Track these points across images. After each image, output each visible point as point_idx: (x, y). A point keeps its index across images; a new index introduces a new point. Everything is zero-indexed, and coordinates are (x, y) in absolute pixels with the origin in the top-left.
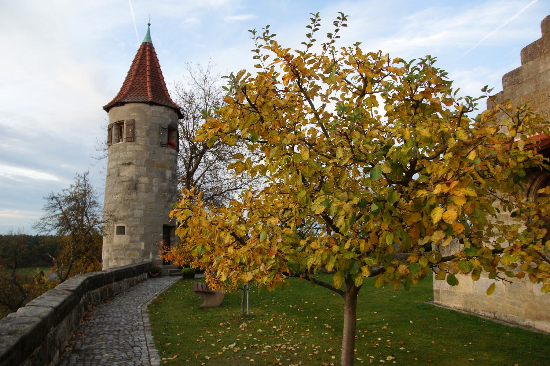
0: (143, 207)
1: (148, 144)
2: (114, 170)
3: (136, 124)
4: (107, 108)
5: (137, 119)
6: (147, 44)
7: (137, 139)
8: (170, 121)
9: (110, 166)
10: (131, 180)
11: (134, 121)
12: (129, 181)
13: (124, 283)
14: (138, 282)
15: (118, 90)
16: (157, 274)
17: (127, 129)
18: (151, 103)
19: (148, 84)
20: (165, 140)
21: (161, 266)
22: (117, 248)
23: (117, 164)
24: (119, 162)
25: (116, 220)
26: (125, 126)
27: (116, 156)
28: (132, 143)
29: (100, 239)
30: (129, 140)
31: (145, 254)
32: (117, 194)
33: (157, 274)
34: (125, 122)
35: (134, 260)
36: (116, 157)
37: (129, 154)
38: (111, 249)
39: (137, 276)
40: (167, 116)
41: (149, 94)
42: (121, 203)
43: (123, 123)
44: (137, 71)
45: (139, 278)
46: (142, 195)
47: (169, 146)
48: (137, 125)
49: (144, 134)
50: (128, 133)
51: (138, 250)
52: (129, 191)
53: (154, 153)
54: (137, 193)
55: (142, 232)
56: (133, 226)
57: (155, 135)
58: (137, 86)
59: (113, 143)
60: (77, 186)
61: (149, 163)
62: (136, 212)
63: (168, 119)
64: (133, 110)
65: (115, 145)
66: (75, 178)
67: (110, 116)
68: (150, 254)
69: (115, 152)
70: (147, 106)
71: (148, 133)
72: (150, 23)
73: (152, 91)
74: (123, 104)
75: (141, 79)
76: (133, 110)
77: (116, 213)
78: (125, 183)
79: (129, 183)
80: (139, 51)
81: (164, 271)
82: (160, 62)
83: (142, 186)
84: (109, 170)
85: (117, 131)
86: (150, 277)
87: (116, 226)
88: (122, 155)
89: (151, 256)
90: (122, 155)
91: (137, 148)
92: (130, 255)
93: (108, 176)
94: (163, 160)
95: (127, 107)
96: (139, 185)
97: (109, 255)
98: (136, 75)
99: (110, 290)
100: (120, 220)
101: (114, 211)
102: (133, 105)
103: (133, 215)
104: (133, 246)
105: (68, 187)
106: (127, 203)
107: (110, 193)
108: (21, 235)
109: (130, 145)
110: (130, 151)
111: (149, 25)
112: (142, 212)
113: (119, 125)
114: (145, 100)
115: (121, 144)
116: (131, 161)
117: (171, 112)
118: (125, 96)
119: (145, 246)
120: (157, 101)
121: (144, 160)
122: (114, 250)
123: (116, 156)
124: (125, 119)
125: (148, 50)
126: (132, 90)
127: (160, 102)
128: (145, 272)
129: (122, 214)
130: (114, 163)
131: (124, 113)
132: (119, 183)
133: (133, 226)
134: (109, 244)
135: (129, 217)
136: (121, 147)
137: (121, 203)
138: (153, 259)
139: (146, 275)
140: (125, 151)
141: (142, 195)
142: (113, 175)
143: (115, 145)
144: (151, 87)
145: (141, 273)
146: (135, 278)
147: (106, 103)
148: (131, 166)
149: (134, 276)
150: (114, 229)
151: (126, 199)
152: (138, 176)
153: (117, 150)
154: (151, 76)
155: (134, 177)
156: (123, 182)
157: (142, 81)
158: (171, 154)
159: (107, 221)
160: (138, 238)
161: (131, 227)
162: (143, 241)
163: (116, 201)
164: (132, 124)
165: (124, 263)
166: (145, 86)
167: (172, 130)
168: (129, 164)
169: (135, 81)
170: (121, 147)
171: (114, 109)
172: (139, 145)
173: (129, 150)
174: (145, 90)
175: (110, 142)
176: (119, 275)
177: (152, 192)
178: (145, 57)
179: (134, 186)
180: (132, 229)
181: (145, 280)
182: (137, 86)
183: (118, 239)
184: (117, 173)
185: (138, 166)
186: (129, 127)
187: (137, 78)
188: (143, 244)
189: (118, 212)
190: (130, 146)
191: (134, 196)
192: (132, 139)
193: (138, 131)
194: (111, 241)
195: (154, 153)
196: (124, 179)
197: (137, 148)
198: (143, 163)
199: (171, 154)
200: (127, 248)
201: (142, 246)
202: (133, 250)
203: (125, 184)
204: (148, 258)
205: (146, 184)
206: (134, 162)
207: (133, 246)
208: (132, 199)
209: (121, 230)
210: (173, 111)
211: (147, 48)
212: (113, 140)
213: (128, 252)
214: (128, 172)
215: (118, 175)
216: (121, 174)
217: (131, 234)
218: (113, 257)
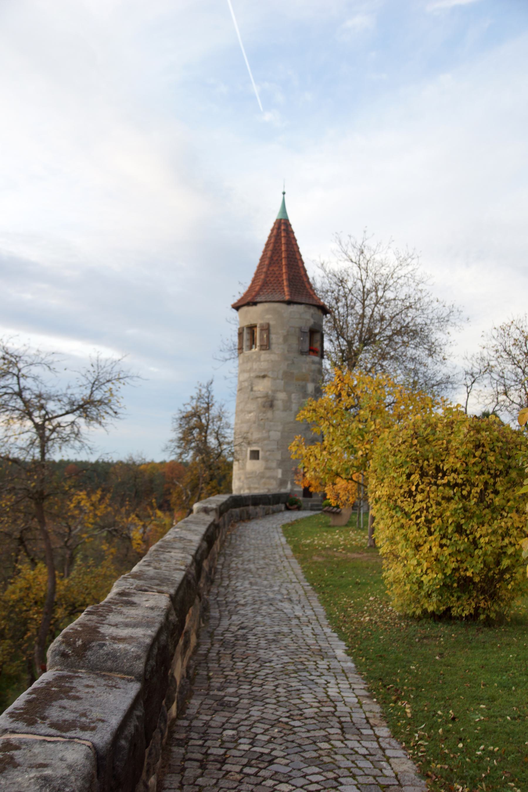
0: (280, 428)
1: (286, 352)
2: (246, 384)
3: (271, 328)
4: (237, 307)
5: (272, 323)
6: (282, 221)
7: (273, 346)
8: (312, 321)
9: (242, 379)
10: (266, 396)
11: (268, 325)
12: (264, 397)
13: (260, 509)
14: (274, 512)
15: (249, 283)
16: (296, 506)
17: (261, 335)
18: (289, 303)
19: (284, 277)
20: (306, 347)
21: (301, 498)
22: (250, 476)
23: (250, 377)
24: (252, 375)
25: (249, 444)
26: (258, 331)
27: (248, 366)
28: (268, 351)
29: (230, 466)
30: (264, 347)
31: (283, 483)
32: (250, 412)
33: (296, 506)
34: (258, 326)
35: (269, 490)
36: (248, 368)
37: (264, 365)
38: (243, 478)
39: (273, 504)
40: (308, 316)
41: (286, 289)
42: (254, 423)
43: (255, 326)
44: (271, 258)
45: (275, 507)
46: (279, 414)
47: (311, 353)
48: (272, 330)
49: (281, 340)
50: (262, 339)
51: (274, 478)
52: (264, 409)
53: (293, 363)
54: (273, 411)
55: (279, 457)
56: (269, 451)
57: (294, 342)
58: (272, 279)
59: (244, 350)
60: (199, 399)
61: (287, 376)
62: (272, 433)
63: (309, 320)
64: (267, 311)
65: (247, 352)
66: (196, 388)
67: (240, 317)
68: (287, 484)
69: (247, 362)
70: (284, 306)
71: (286, 339)
72: (286, 191)
73: (289, 286)
74: (255, 304)
75: (275, 269)
76: (267, 311)
77: (249, 435)
78: (259, 399)
79: (264, 399)
80: (272, 230)
81: (304, 505)
82: (299, 243)
83: (279, 404)
84: (240, 382)
85: (249, 335)
86: (288, 509)
87: (249, 449)
88: (255, 366)
89: (289, 486)
90: (255, 366)
91: (273, 357)
92: (265, 484)
93: (240, 390)
94: (304, 371)
95: (259, 308)
96: (276, 403)
97: (241, 484)
98: (270, 265)
99: (247, 513)
100: (255, 443)
101: (247, 433)
102: (267, 305)
103: (269, 437)
104: (268, 474)
105: (188, 400)
106: (262, 423)
107: (242, 411)
108: (103, 462)
109: (265, 353)
110: (264, 361)
111: (284, 193)
112: (279, 434)
113: (252, 328)
114: (281, 299)
115: (254, 353)
116: (266, 373)
117: (312, 310)
118: (258, 294)
119: (283, 474)
120: (297, 299)
121: (281, 372)
122: (247, 478)
123: (248, 366)
124: (259, 322)
125: (284, 230)
126: (265, 284)
127: (299, 301)
128: (282, 503)
129: (256, 436)
130: (246, 375)
131: (256, 314)
132: (252, 399)
133: (269, 451)
134: (241, 471)
135: (264, 439)
136: (255, 357)
137: (254, 423)
138: (292, 490)
139: (283, 507)
140: (259, 361)
141: (279, 414)
142: (246, 390)
143: (247, 352)
144: (289, 280)
145: (277, 503)
146: (271, 507)
147: (235, 300)
148: (266, 379)
149: (270, 504)
150: (246, 455)
151: (260, 418)
152: (275, 391)
153: (249, 359)
154: (288, 266)
155: (270, 392)
156: (257, 398)
157: (277, 273)
158: (313, 362)
159: (240, 445)
160: (274, 465)
161: (267, 451)
162: (280, 468)
163: (248, 421)
164: (267, 329)
165: (259, 490)
166: (280, 279)
167: (314, 334)
168: (264, 377)
169: (269, 272)
170: (255, 357)
171: (245, 309)
172: (275, 353)
173: (263, 360)
174: (281, 283)
175: (241, 349)
176: (256, 500)
177: (291, 410)
178: (280, 239)
179: (270, 403)
180: (268, 453)
181: (281, 511)
182: (272, 279)
183: (251, 465)
184: (250, 387)
185: (274, 379)
186: (263, 332)
187: (271, 269)
188: (280, 471)
189: (252, 434)
190: (264, 355)
191: (269, 414)
192: (266, 346)
193: (273, 337)
194: (243, 468)
195: (293, 363)
196: (258, 394)
197: (273, 357)
198: (280, 376)
199: (313, 362)
200: (262, 476)
201: (279, 473)
202: (269, 478)
203: (260, 400)
204: (286, 488)
205: (283, 401)
206: (270, 374)
207: (268, 474)
208: (268, 419)
209: (255, 455)
210: (315, 308)
211: (283, 227)
212: (244, 347)
213: (263, 480)
214: (263, 387)
215: (252, 390)
216: (255, 388)
217: (266, 460)
218: (245, 486)
